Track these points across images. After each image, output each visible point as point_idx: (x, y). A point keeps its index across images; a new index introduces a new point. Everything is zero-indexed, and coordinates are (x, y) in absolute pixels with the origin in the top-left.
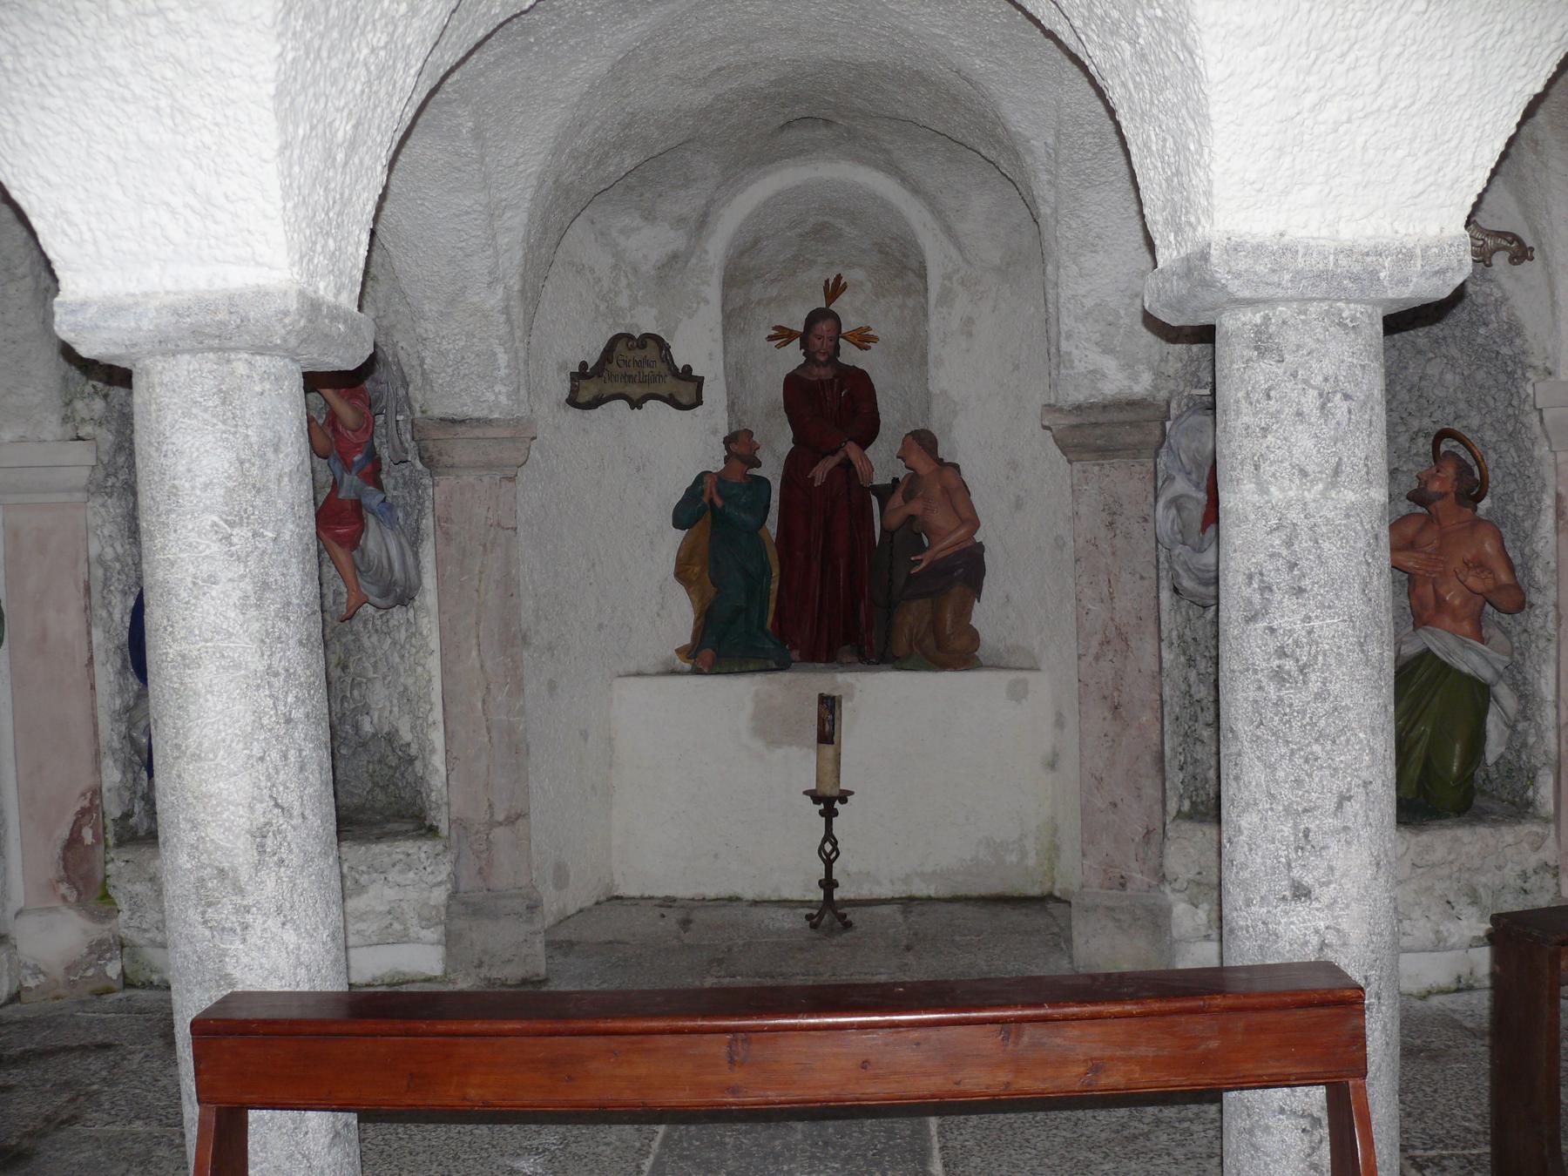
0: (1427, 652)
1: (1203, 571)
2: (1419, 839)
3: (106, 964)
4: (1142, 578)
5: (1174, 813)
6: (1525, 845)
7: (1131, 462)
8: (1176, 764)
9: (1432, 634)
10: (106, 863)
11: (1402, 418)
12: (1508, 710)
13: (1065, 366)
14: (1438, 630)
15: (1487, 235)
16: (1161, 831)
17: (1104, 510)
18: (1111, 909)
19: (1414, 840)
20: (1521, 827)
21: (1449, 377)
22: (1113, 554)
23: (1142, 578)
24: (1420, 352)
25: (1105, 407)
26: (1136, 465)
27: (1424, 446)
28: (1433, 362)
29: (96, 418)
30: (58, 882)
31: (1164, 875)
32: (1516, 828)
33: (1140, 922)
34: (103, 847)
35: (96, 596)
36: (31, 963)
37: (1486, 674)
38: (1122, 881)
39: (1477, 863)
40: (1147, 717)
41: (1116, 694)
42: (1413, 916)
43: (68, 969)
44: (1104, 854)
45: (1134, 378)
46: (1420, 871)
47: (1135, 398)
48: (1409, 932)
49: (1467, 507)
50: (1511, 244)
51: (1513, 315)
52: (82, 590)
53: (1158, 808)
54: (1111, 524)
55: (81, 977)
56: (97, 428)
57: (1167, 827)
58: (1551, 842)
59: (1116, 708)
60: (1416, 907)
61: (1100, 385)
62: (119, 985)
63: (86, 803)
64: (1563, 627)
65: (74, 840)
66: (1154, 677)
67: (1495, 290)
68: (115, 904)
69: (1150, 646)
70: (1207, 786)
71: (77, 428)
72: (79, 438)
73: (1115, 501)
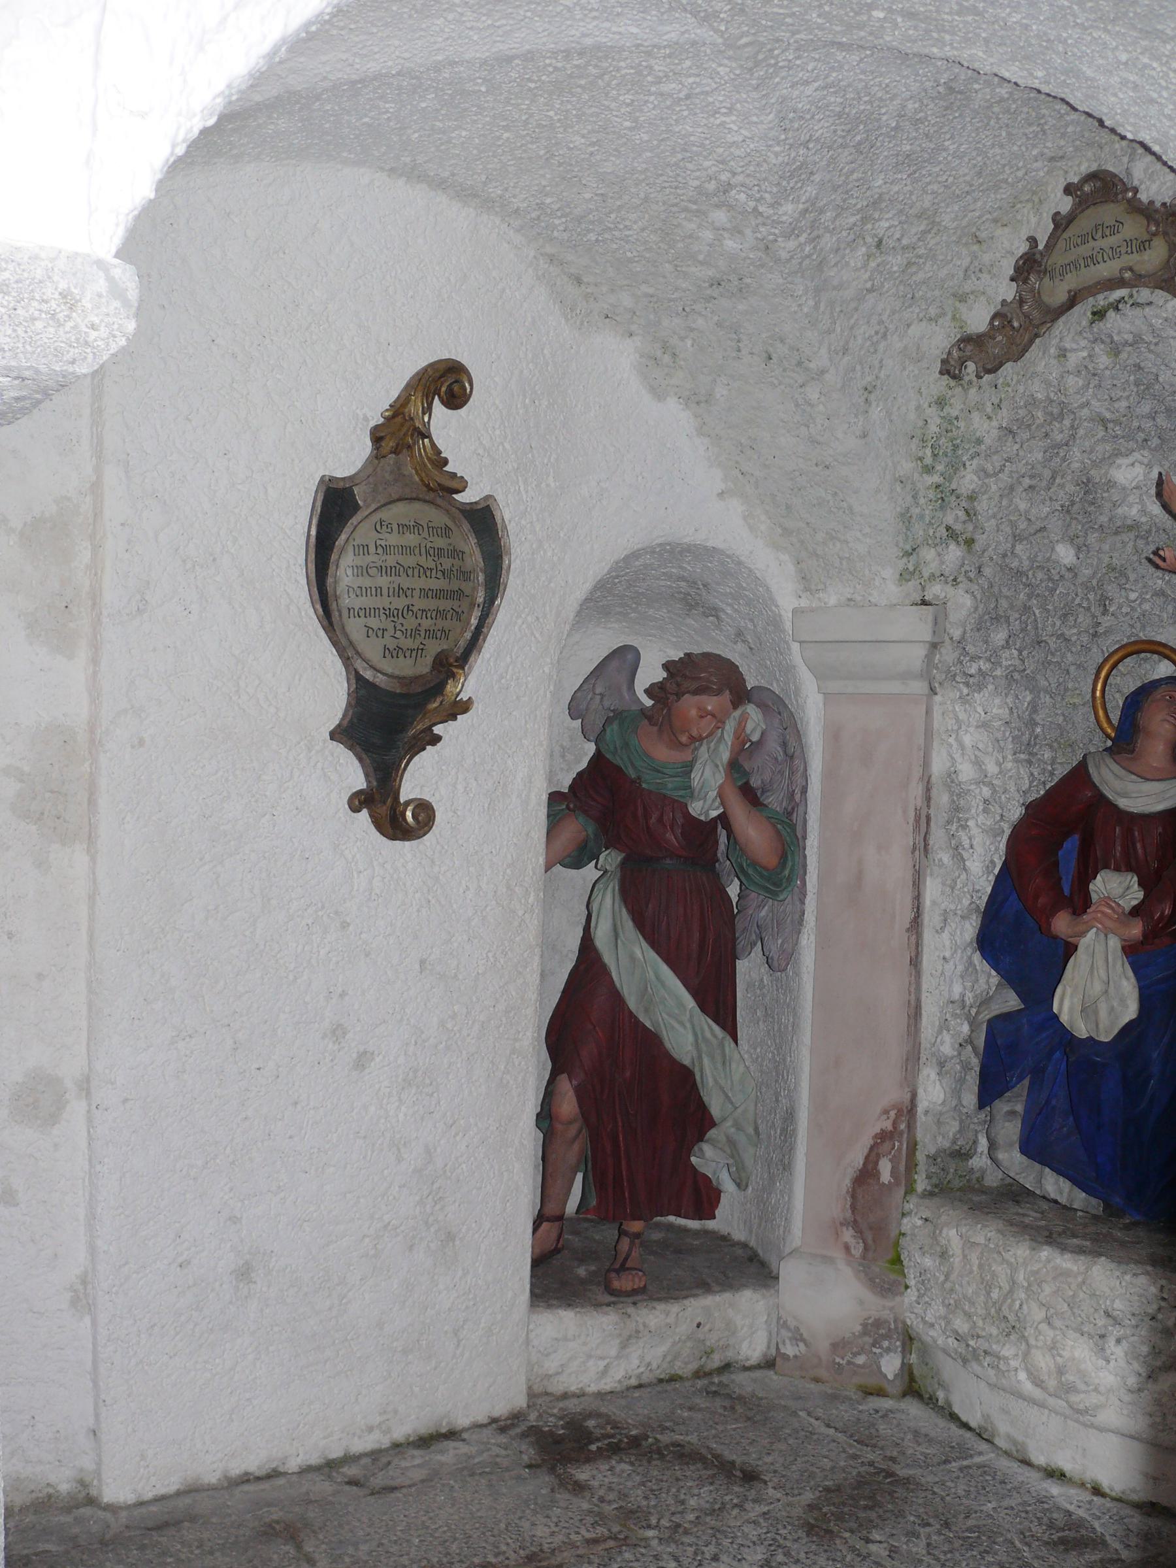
3: (881, 1355)
10: (903, 1215)
29: (947, 574)
30: (842, 1224)
34: (902, 1192)
35: (938, 836)
36: (792, 1323)
43: (835, 1346)
52: (912, 820)
55: (849, 1363)
56: (949, 589)
62: (895, 1389)
63: (888, 1125)
65: (866, 1175)
68: (905, 1276)
71: (923, 589)
72: (924, 603)
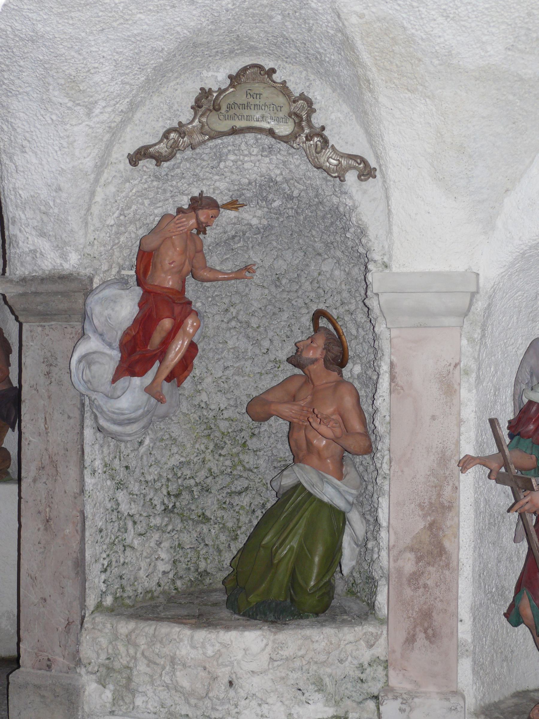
0: (298, 486)
1: (118, 414)
2: (276, 637)
4: (69, 417)
5: (92, 608)
6: (362, 642)
7: (65, 324)
8: (98, 567)
9: (302, 469)
11: (306, 304)
12: (358, 532)
13: (13, 246)
14: (307, 467)
15: (342, 157)
16: (78, 622)
17: (43, 362)
18: (38, 687)
19: (272, 637)
20: (360, 628)
21: (337, 273)
22: (49, 397)
23: (69, 417)
24: (320, 254)
25: (43, 280)
26: (68, 327)
27: (306, 321)
28: (326, 262)
31: (80, 659)
32: (356, 629)
33: (59, 699)
37: (340, 503)
38: (49, 663)
39: (322, 658)
40: (68, 530)
41: (48, 510)
42: (270, 701)
44: (36, 641)
45: (64, 256)
46: (276, 664)
47: (64, 273)
48: (267, 714)
49: (334, 371)
50: (360, 164)
51: (361, 220)
53: (76, 604)
54: (48, 373)
57: (86, 619)
58: (382, 641)
59: (48, 521)
60: (272, 694)
61: (39, 262)
64: (393, 468)
66: (75, 498)
67: (348, 200)
69: (73, 472)
70: (136, 583)
73: (52, 356)
